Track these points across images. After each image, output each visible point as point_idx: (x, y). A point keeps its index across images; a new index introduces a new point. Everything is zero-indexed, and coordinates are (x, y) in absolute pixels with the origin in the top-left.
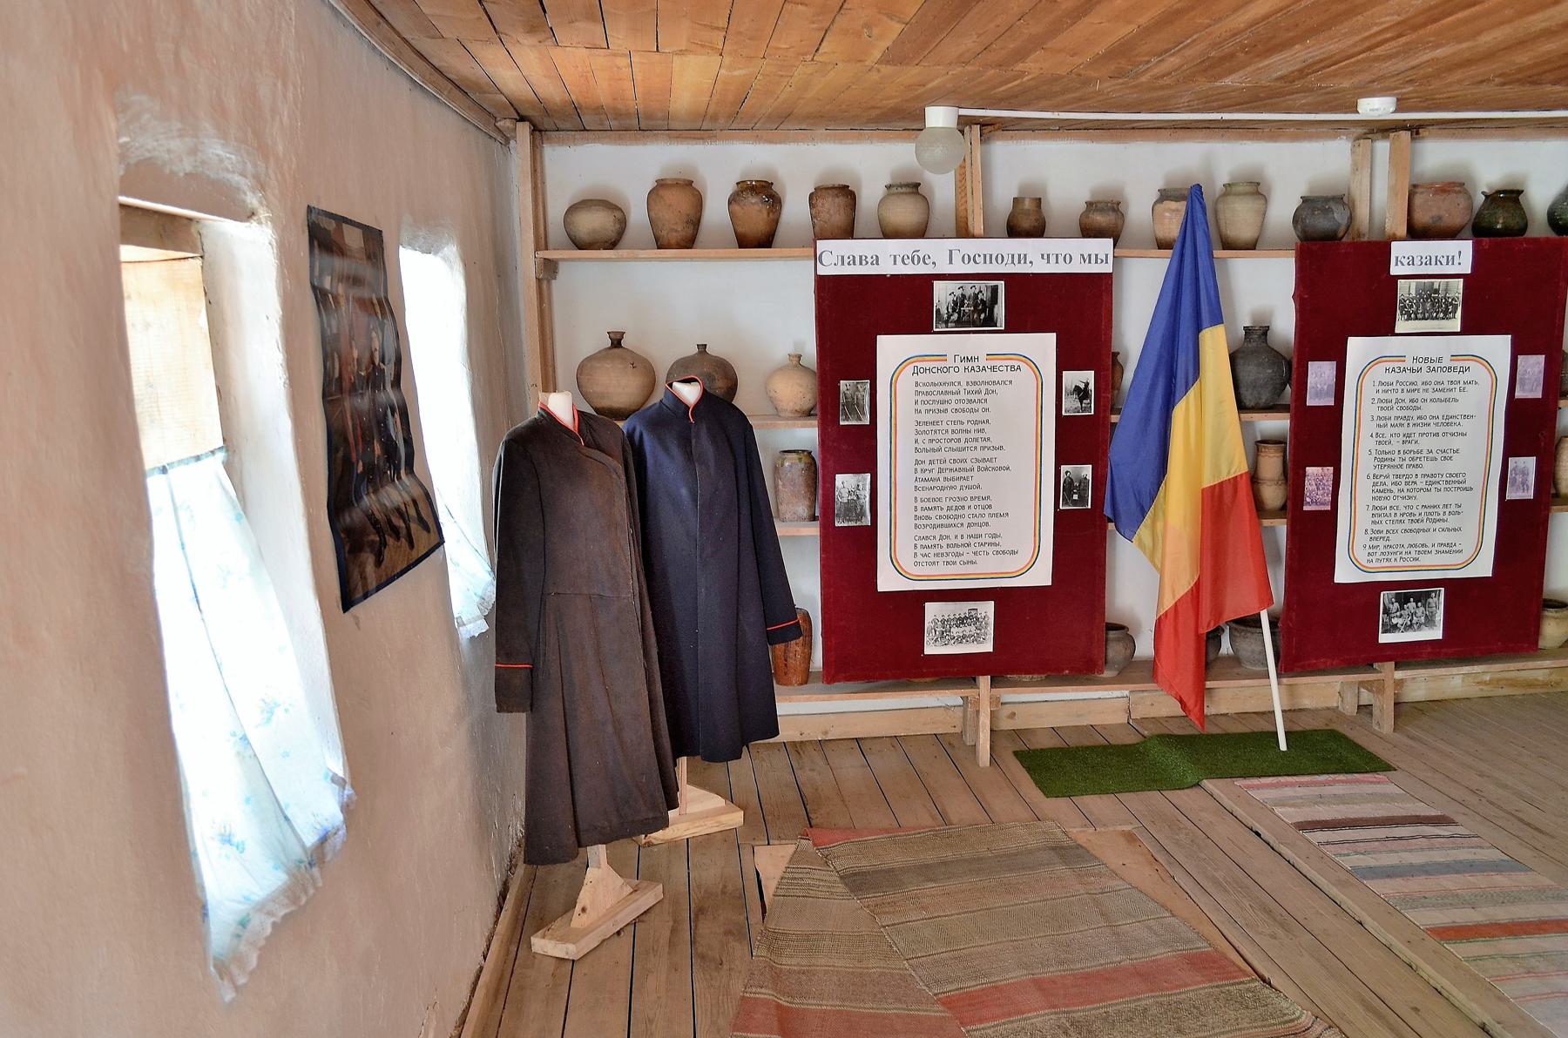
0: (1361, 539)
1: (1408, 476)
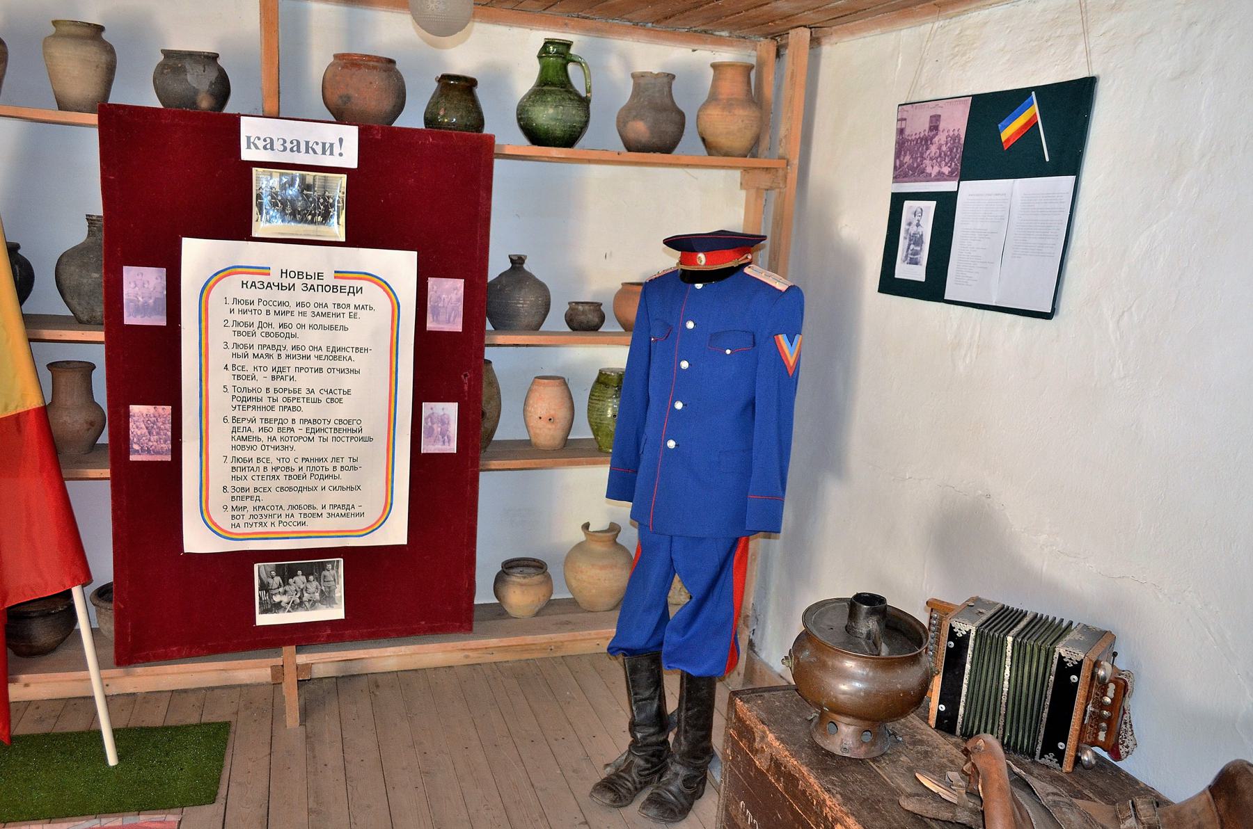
0: (217, 499)
1: (282, 421)
